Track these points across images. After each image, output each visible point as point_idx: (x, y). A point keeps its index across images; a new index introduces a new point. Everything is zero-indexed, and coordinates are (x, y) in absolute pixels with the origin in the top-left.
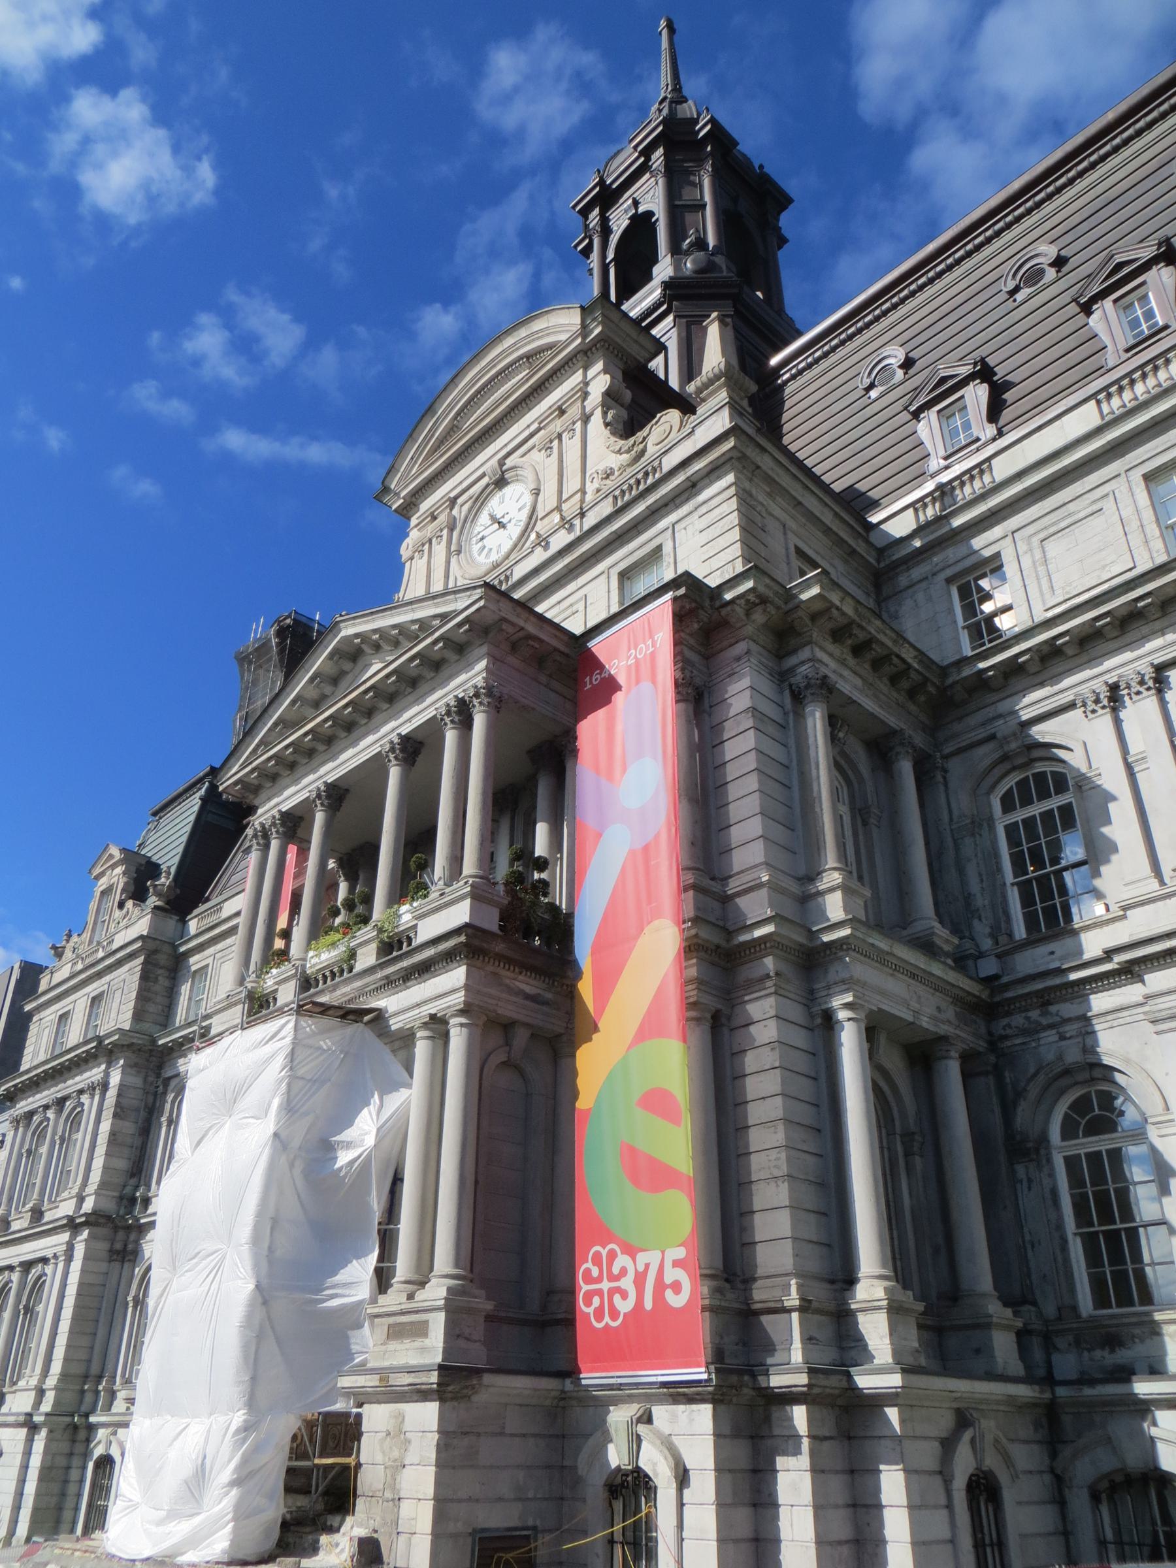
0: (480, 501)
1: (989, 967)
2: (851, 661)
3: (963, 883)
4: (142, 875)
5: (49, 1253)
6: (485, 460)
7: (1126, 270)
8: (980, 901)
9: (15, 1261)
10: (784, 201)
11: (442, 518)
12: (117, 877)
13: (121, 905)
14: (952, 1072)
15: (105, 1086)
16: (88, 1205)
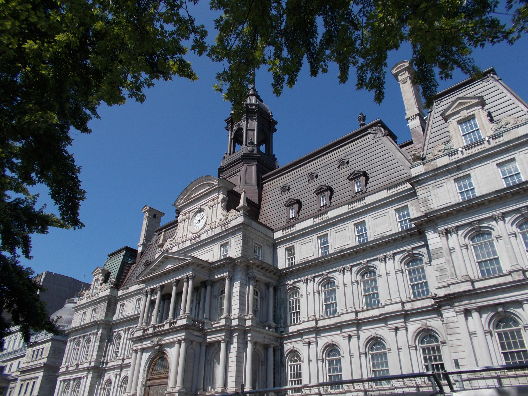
0: (196, 214)
1: (282, 329)
2: (261, 271)
3: (281, 312)
4: (107, 276)
5: (82, 376)
6: (197, 205)
7: (322, 190)
8: (283, 316)
9: (71, 378)
10: (276, 123)
11: (187, 215)
12: (101, 277)
13: (101, 284)
14: (271, 350)
15: (97, 334)
16: (93, 364)
